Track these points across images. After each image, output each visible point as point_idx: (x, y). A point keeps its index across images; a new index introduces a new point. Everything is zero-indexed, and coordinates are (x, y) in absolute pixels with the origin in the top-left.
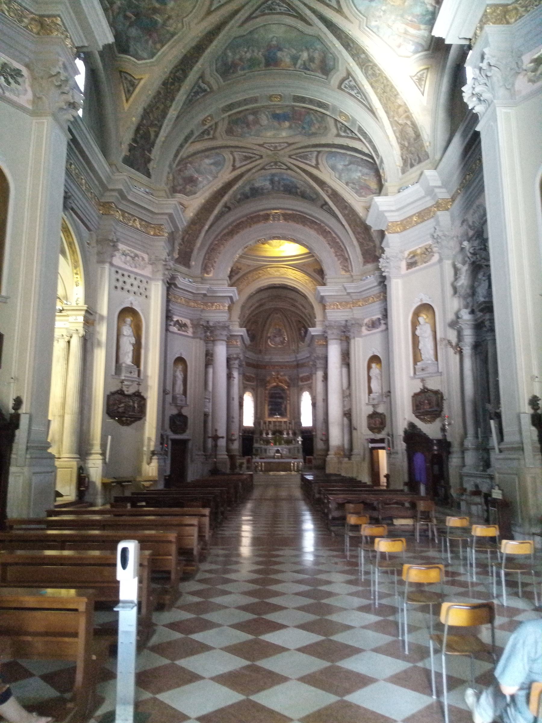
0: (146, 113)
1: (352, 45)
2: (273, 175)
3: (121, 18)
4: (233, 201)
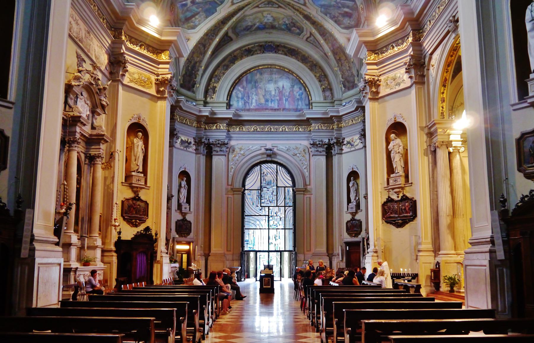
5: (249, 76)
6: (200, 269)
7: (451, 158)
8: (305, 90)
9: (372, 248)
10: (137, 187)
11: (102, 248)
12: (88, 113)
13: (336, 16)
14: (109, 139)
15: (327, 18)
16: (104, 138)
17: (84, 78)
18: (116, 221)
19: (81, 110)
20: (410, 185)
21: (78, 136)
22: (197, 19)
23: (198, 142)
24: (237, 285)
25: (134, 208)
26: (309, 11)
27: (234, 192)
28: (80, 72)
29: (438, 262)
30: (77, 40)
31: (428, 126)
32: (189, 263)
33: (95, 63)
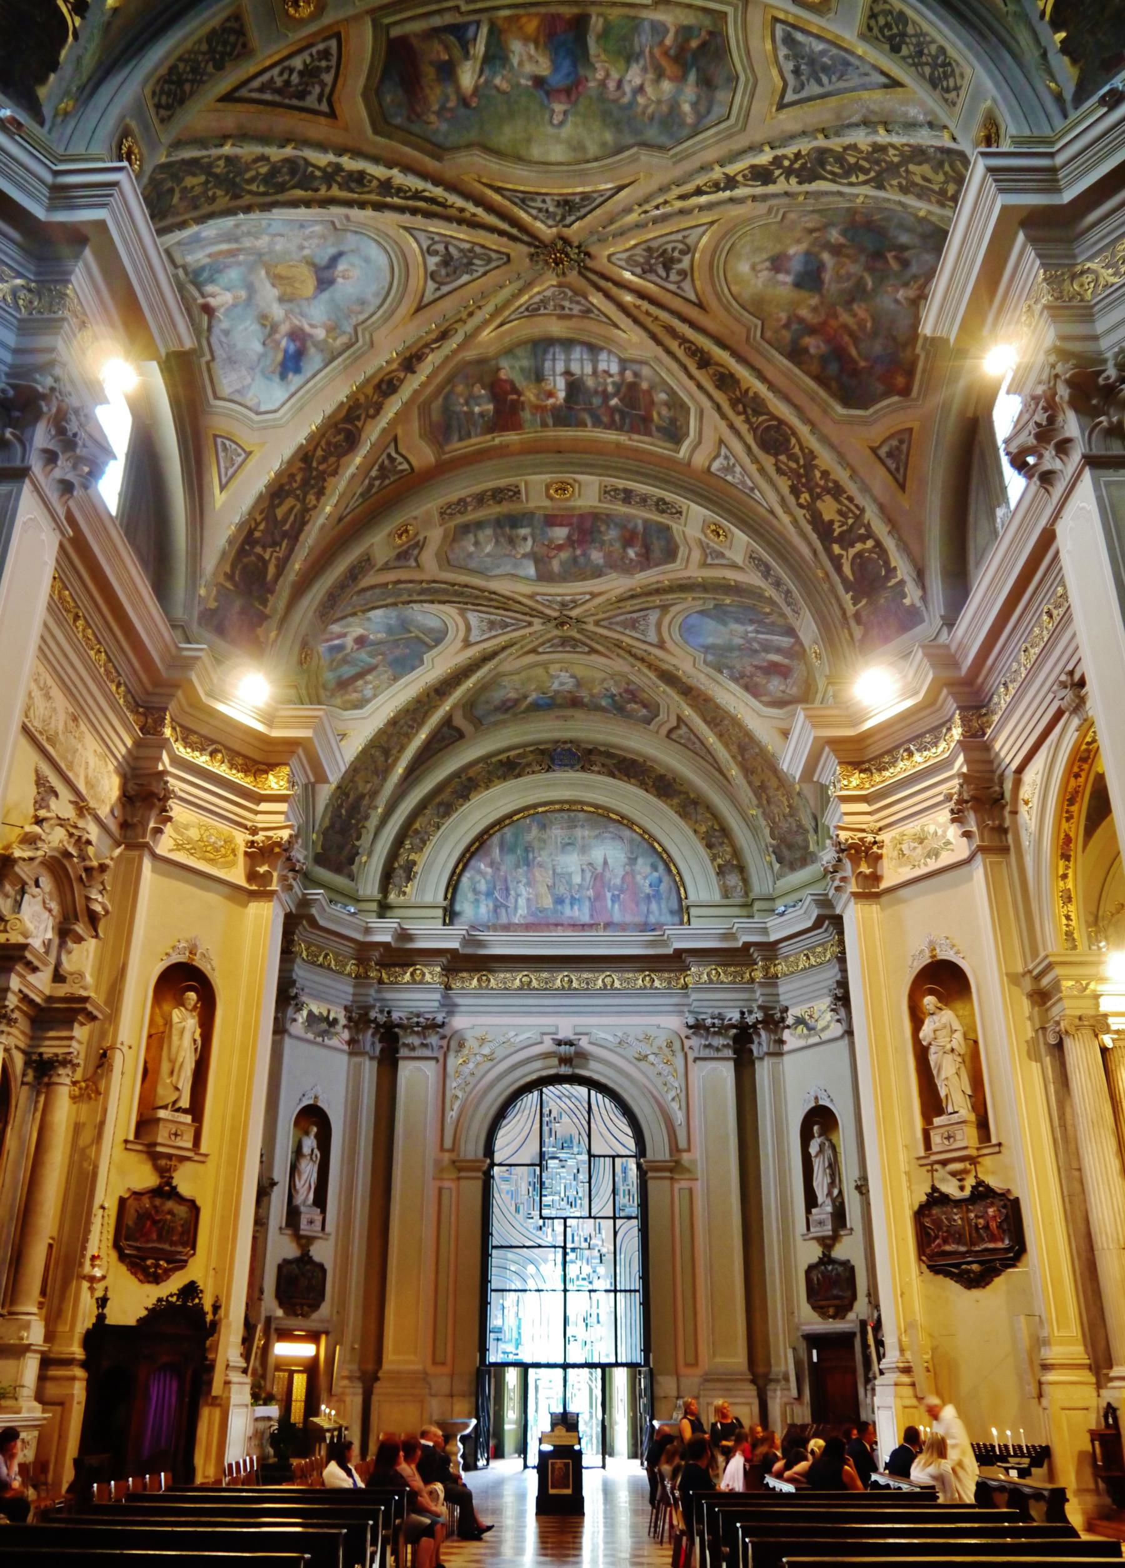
3: (914, 269)
5: (508, 832)
6: (344, 1423)
7: (1112, 1066)
8: (669, 871)
9: (892, 1357)
10: (170, 1157)
11: (42, 1353)
12: (50, 935)
14: (101, 1012)
16: (85, 1009)
17: (50, 838)
18: (97, 1262)
19: (30, 926)
20: (996, 1149)
21: (12, 1001)
23: (359, 1019)
24: (464, 1485)
25: (155, 1222)
26: (674, 661)
27: (460, 1170)
28: (39, 821)
29: (1109, 1404)
30: (42, 739)
31: (1030, 972)
32: (312, 1407)
33: (83, 799)
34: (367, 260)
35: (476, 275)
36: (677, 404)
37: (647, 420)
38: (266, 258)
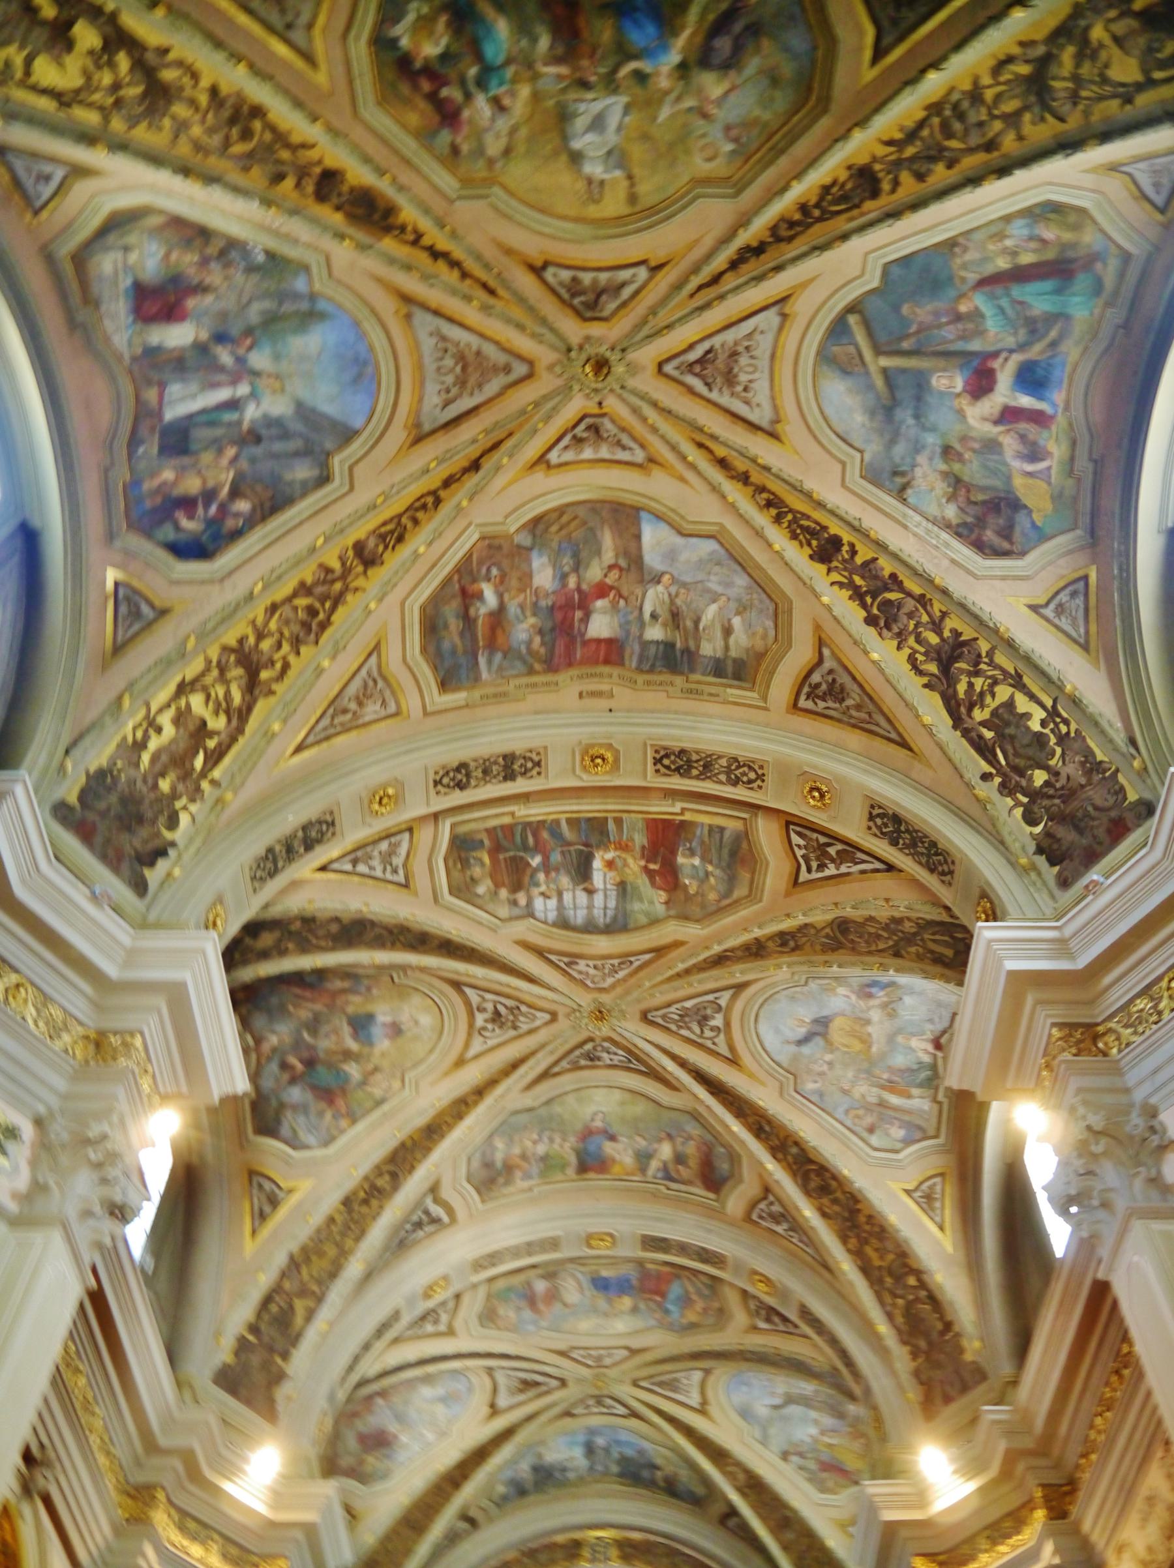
0: (293, 1265)
1: (767, 1128)
2: (592, 1432)
3: (274, 1067)
4: (485, 1503)
13: (214, 266)
15: (259, 243)
22: (1005, 251)
26: (370, 263)
34: (777, 1031)
35: (678, 1006)
36: (463, 889)
37: (496, 849)
38: (865, 1065)
